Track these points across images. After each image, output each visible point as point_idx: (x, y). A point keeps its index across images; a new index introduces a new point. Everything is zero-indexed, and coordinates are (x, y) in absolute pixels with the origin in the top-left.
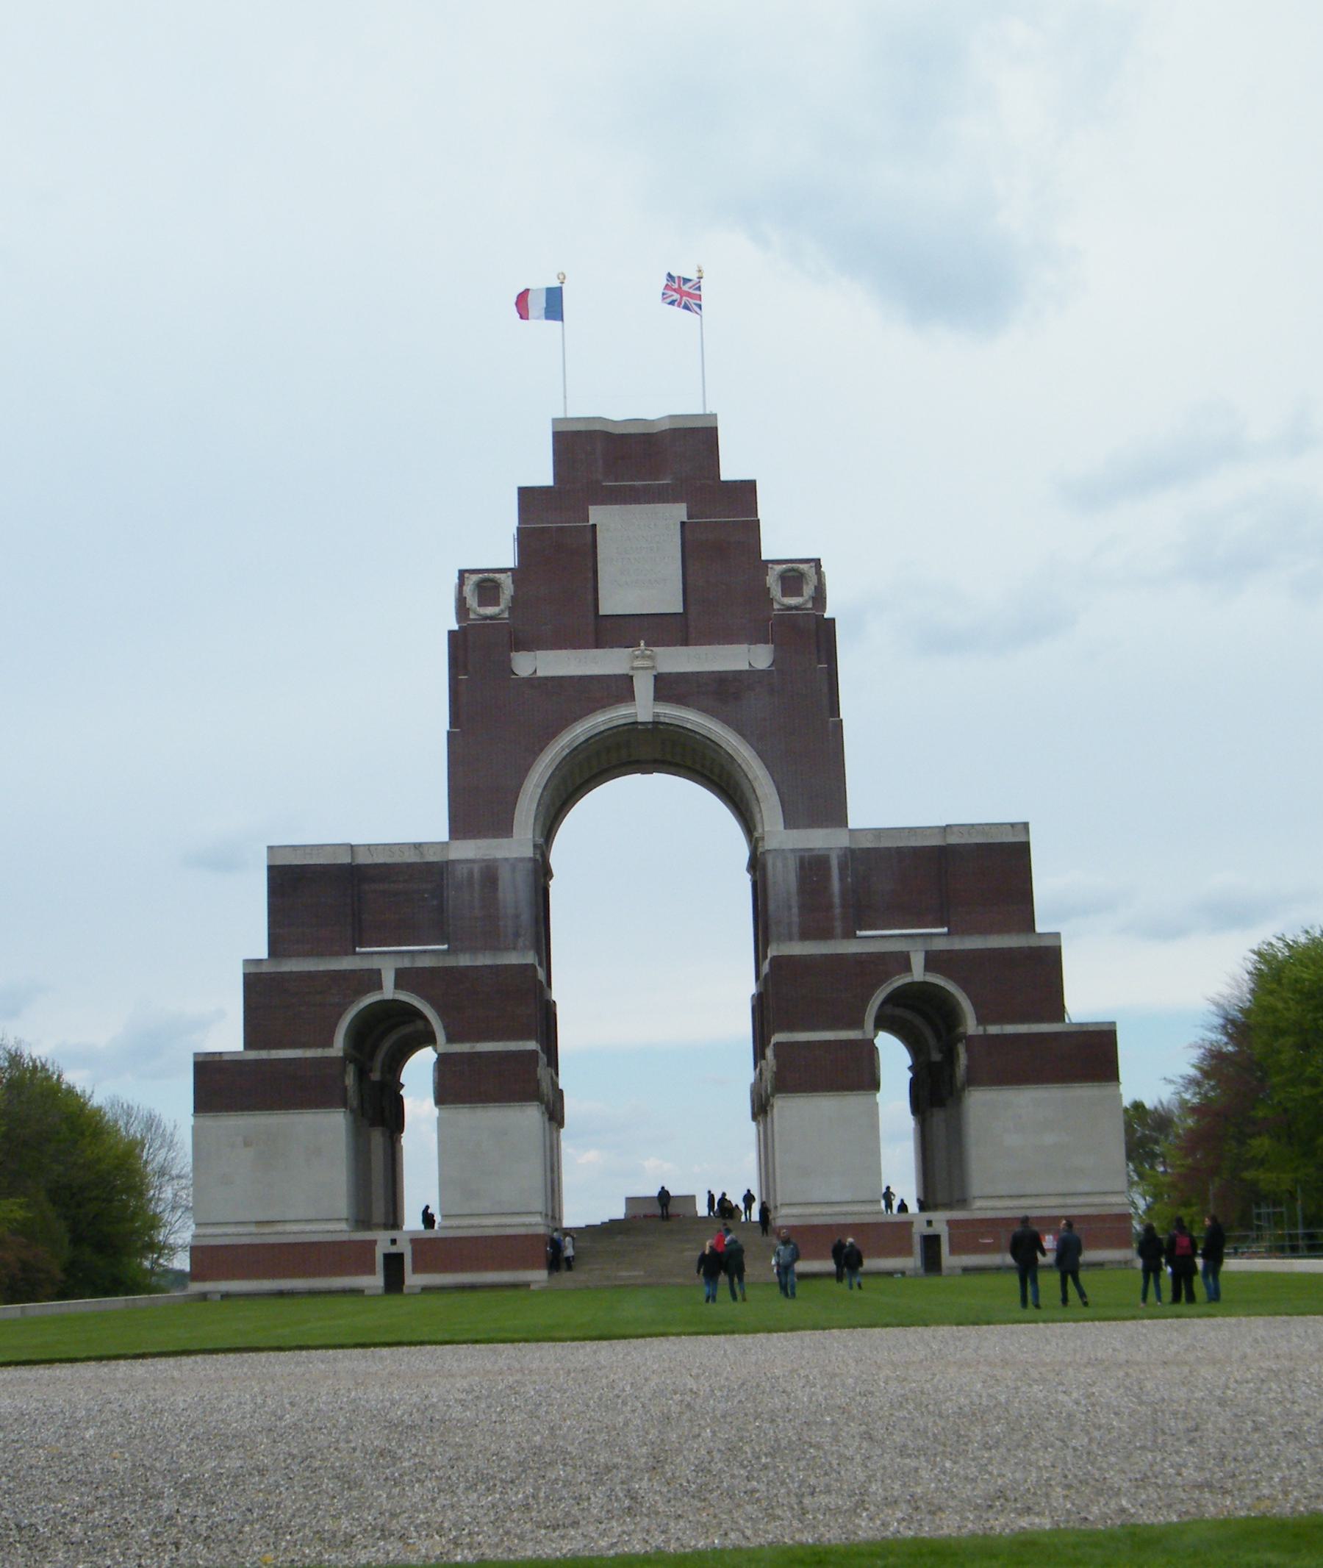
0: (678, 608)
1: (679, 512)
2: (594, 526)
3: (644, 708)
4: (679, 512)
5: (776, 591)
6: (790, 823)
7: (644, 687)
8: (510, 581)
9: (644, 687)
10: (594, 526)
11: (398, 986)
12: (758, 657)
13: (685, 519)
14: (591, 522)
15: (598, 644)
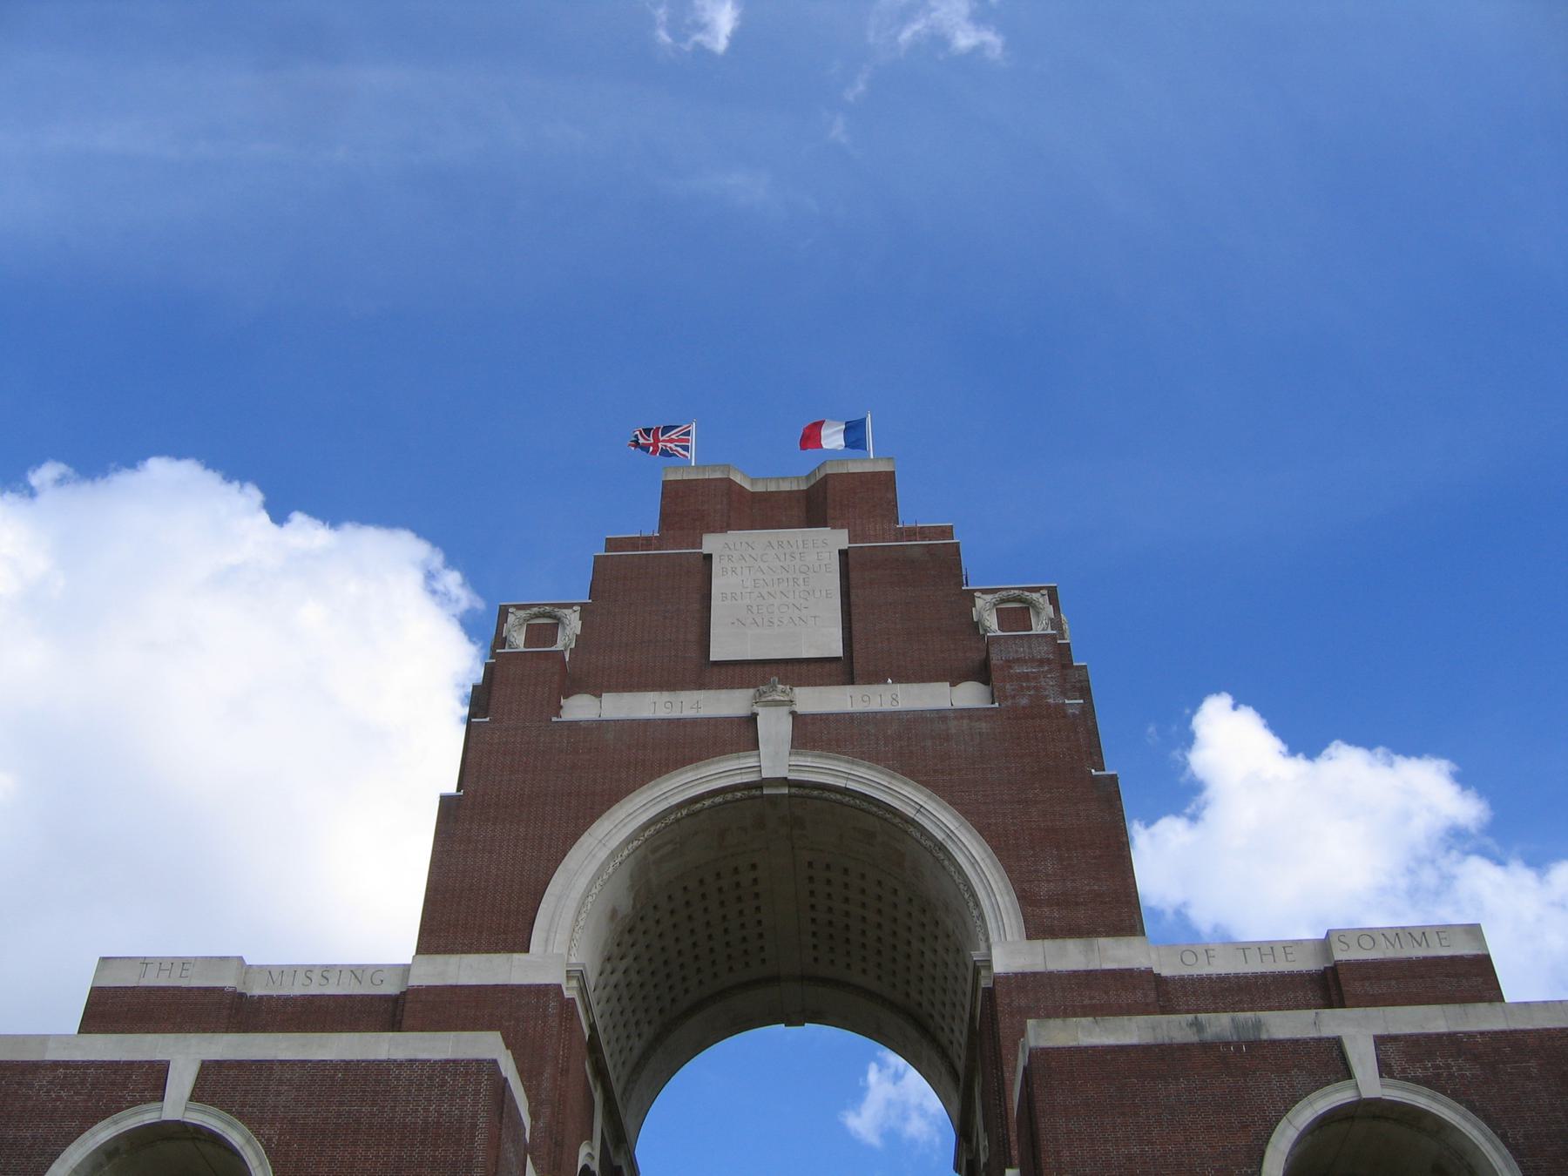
0: (836, 650)
1: (839, 538)
2: (708, 557)
3: (775, 757)
4: (839, 538)
5: (991, 622)
6: (1036, 929)
7: (774, 727)
8: (577, 615)
9: (774, 727)
10: (708, 557)
11: (200, 1094)
12: (969, 695)
13: (845, 545)
14: (705, 550)
15: (701, 685)
